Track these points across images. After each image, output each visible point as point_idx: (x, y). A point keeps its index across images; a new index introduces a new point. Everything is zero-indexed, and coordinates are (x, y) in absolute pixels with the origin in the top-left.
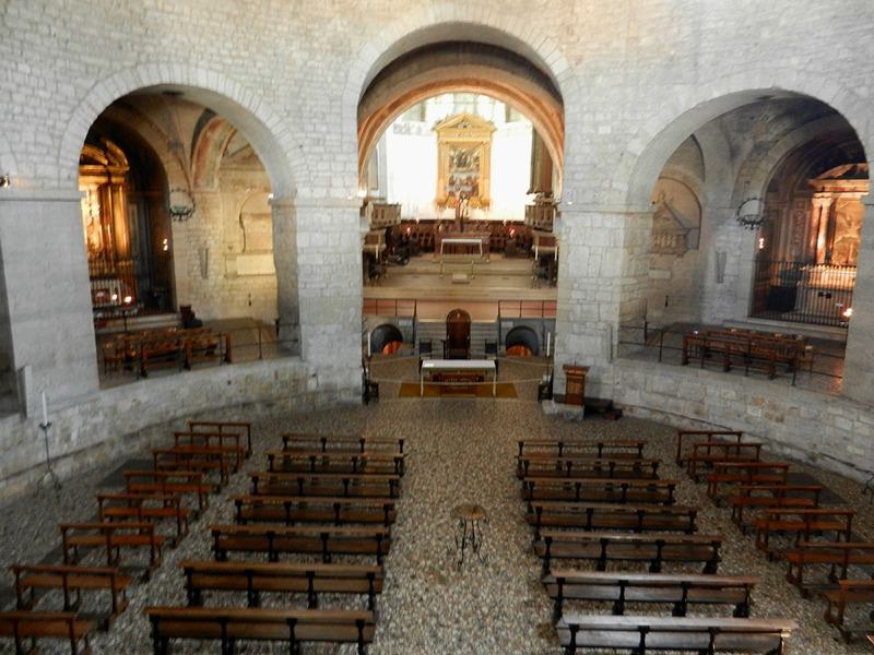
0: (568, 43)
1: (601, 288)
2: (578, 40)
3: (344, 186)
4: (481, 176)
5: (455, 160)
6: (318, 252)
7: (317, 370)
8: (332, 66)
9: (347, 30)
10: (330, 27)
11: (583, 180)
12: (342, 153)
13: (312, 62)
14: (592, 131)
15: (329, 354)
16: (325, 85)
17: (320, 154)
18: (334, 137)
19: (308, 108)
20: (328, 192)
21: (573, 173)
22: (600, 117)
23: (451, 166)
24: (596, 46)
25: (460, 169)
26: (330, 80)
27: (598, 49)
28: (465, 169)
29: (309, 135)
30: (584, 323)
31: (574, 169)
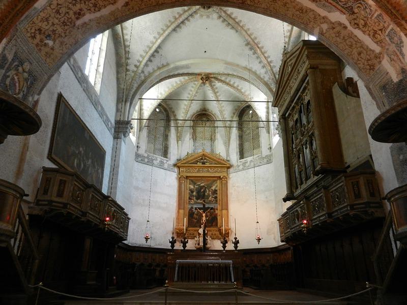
4: (219, 208)
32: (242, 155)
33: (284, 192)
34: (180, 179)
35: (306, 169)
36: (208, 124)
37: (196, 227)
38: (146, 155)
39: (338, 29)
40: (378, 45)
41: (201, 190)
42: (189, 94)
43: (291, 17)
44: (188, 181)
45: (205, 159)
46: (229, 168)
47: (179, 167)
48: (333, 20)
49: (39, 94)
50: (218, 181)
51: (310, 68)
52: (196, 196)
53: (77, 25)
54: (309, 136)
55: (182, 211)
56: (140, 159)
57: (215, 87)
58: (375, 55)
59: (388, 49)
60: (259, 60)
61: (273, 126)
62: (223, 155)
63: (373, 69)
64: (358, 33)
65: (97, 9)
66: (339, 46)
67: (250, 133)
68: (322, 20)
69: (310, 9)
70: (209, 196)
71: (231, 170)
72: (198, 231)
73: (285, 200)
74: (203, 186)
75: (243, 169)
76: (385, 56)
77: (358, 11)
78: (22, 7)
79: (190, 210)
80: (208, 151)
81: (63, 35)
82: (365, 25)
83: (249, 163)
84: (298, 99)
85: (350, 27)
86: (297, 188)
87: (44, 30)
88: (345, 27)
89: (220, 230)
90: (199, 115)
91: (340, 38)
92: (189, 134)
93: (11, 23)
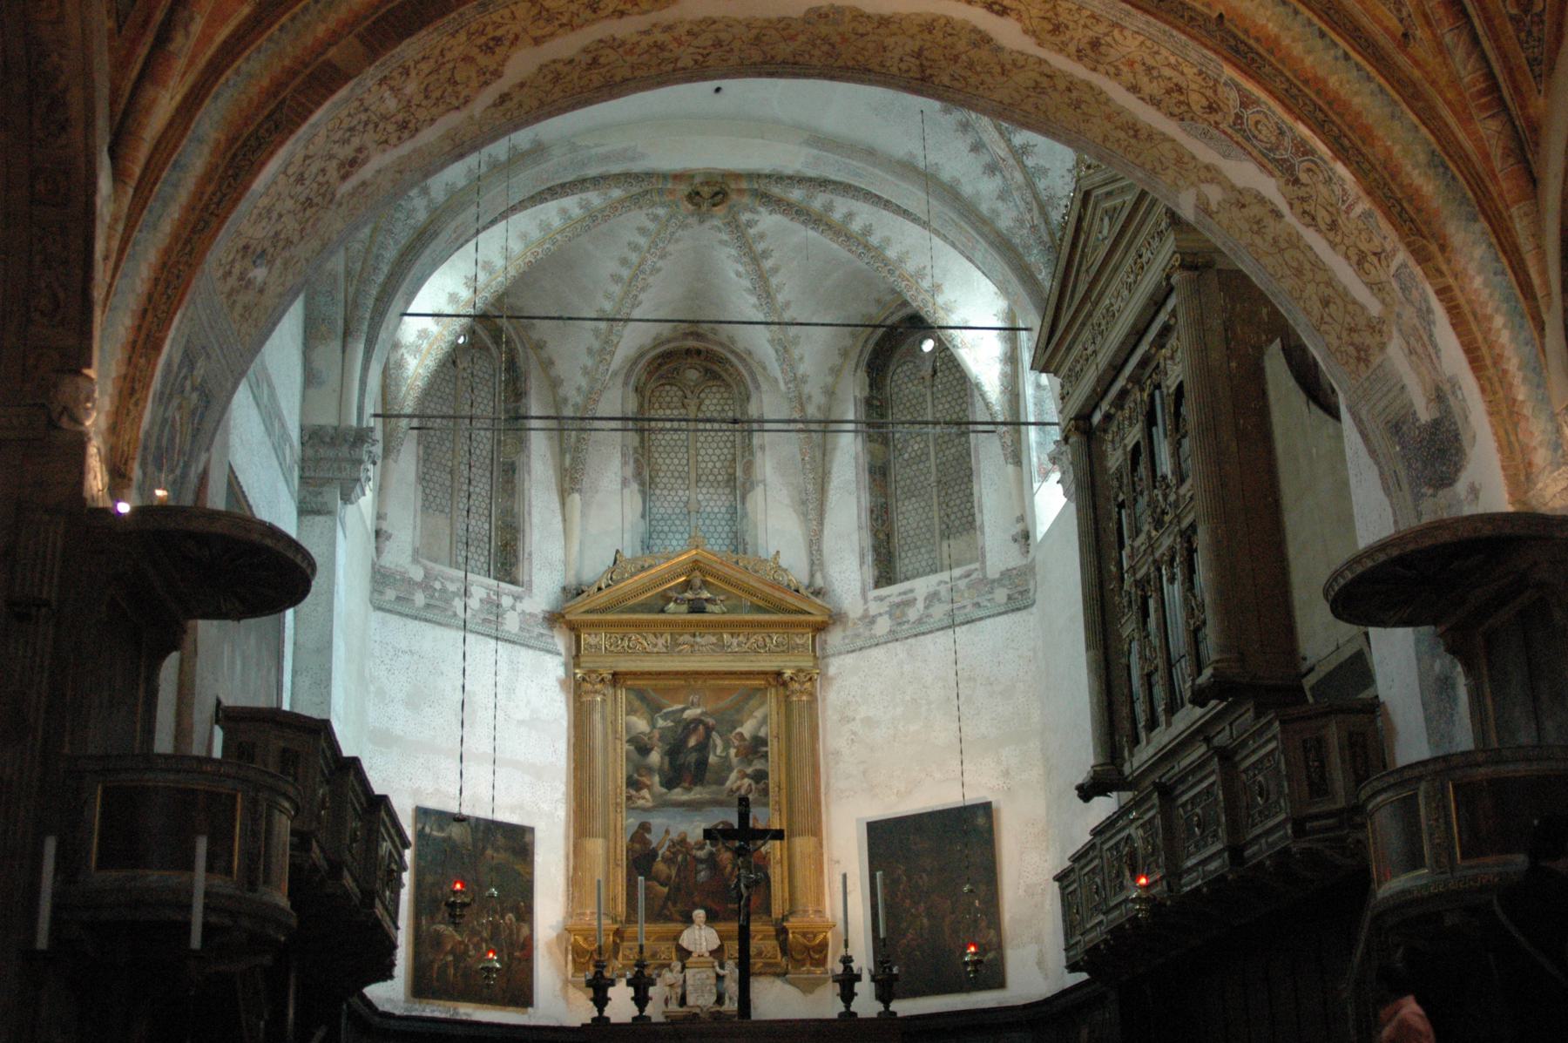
5: (655, 757)
23: (633, 783)
25: (678, 794)
28: (697, 794)
32: (886, 568)
33: (1083, 758)
34: (578, 690)
35: (1170, 665)
36: (712, 403)
37: (669, 919)
38: (417, 574)
39: (1255, 210)
40: (1374, 295)
41: (684, 741)
42: (624, 262)
43: (1099, 140)
44: (622, 695)
45: (705, 584)
46: (820, 628)
47: (574, 629)
48: (1240, 184)
49: (208, 450)
50: (772, 696)
51: (1183, 266)
52: (661, 771)
53: (338, 196)
54: (1182, 533)
55: (596, 847)
56: (390, 594)
57: (752, 231)
58: (1369, 319)
59: (1399, 316)
60: (969, 139)
61: (1039, 443)
62: (795, 564)
63: (1367, 362)
64: (1311, 236)
65: (406, 134)
66: (1262, 261)
67: (922, 457)
68: (1203, 174)
69: (1163, 134)
70: (726, 766)
71: (835, 638)
72: (676, 937)
73: (1087, 792)
74: (697, 721)
75: (893, 637)
76: (1395, 334)
77: (1309, 182)
78: (214, 194)
79: (632, 840)
80: (715, 547)
81: (296, 239)
82: (1333, 226)
83: (920, 605)
84: (1144, 363)
85: (1290, 218)
86: (1136, 741)
87: (255, 242)
88: (1278, 215)
89: (782, 932)
90: (668, 356)
91: (1264, 241)
92: (617, 461)
93: (191, 253)
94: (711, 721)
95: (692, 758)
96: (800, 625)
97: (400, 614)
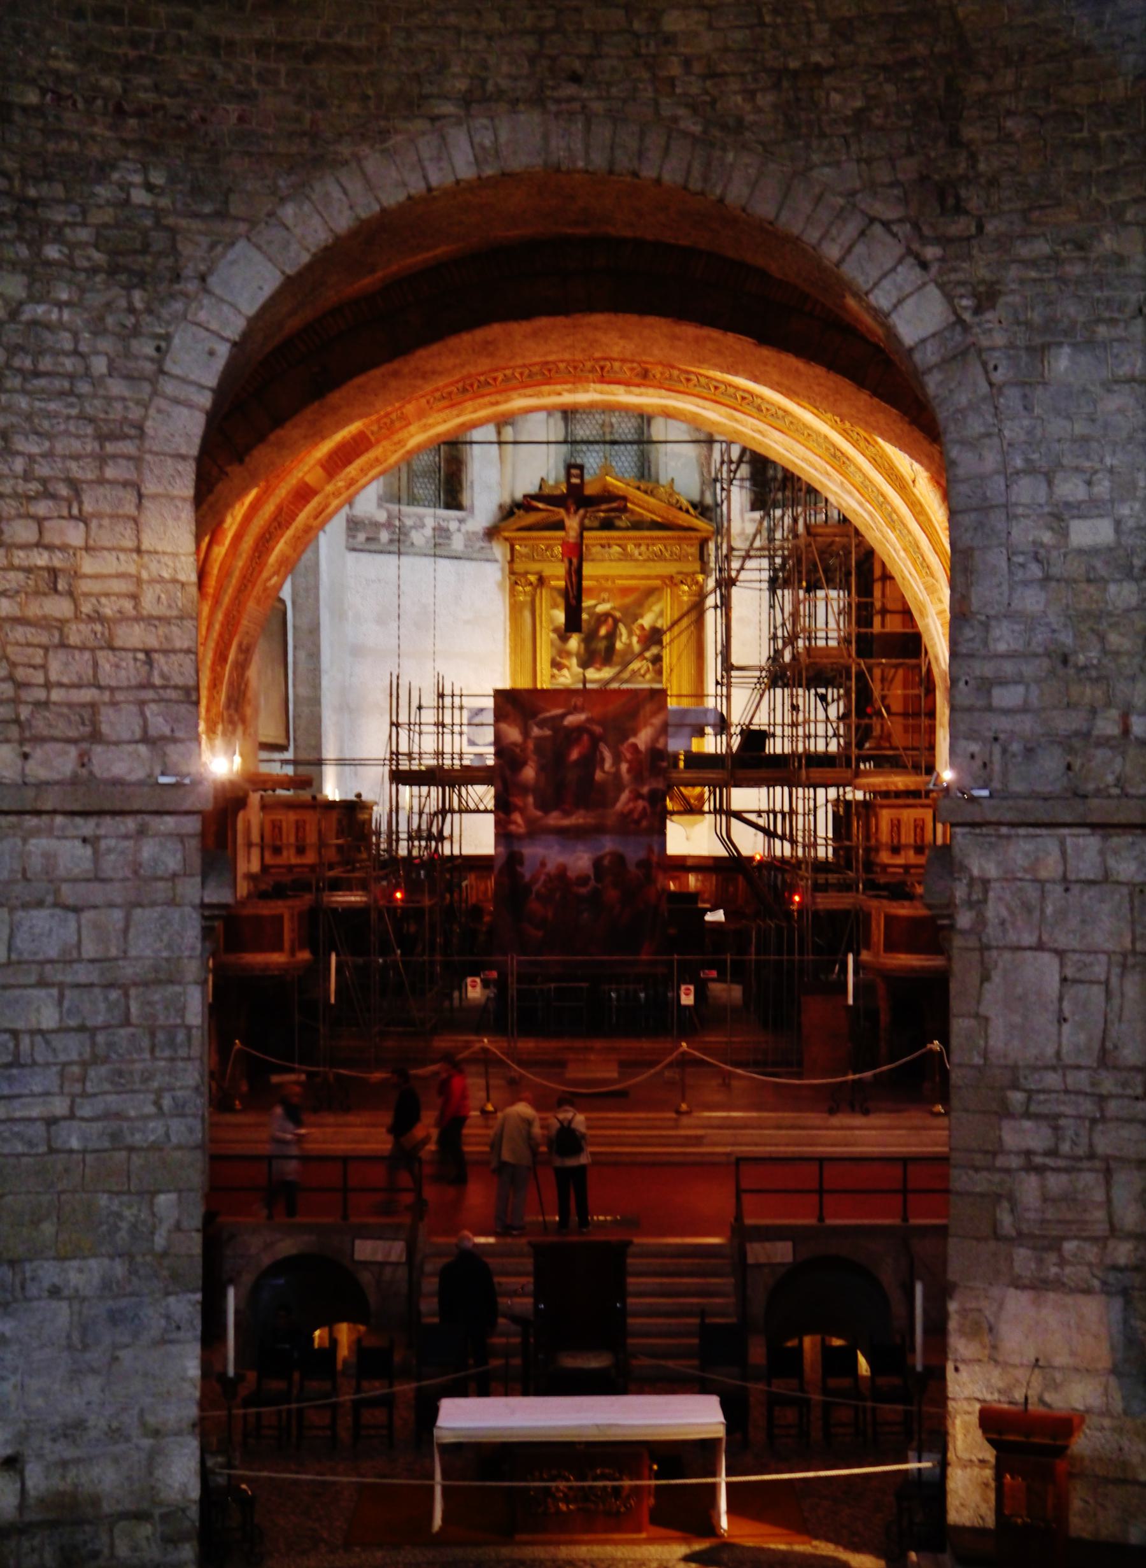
0: (943, 240)
1: (1112, 1107)
2: (980, 228)
3: (146, 739)
6: (42, 983)
7: (23, 1437)
8: (110, 321)
9: (164, 202)
10: (103, 192)
11: (1025, 709)
12: (139, 619)
13: (41, 309)
14: (1047, 537)
15: (76, 1374)
16: (84, 388)
17: (61, 624)
18: (108, 563)
19: (19, 465)
20: (84, 760)
21: (985, 686)
22: (1071, 489)
24: (1042, 248)
26: (100, 365)
27: (1055, 258)
29: (20, 557)
30: (1054, 1245)
31: (987, 669)
38: (381, 516)
41: (597, 630)
52: (578, 655)
56: (361, 537)
74: (607, 615)
94: (618, 614)
95: (602, 645)
96: (691, 538)
97: (370, 551)
